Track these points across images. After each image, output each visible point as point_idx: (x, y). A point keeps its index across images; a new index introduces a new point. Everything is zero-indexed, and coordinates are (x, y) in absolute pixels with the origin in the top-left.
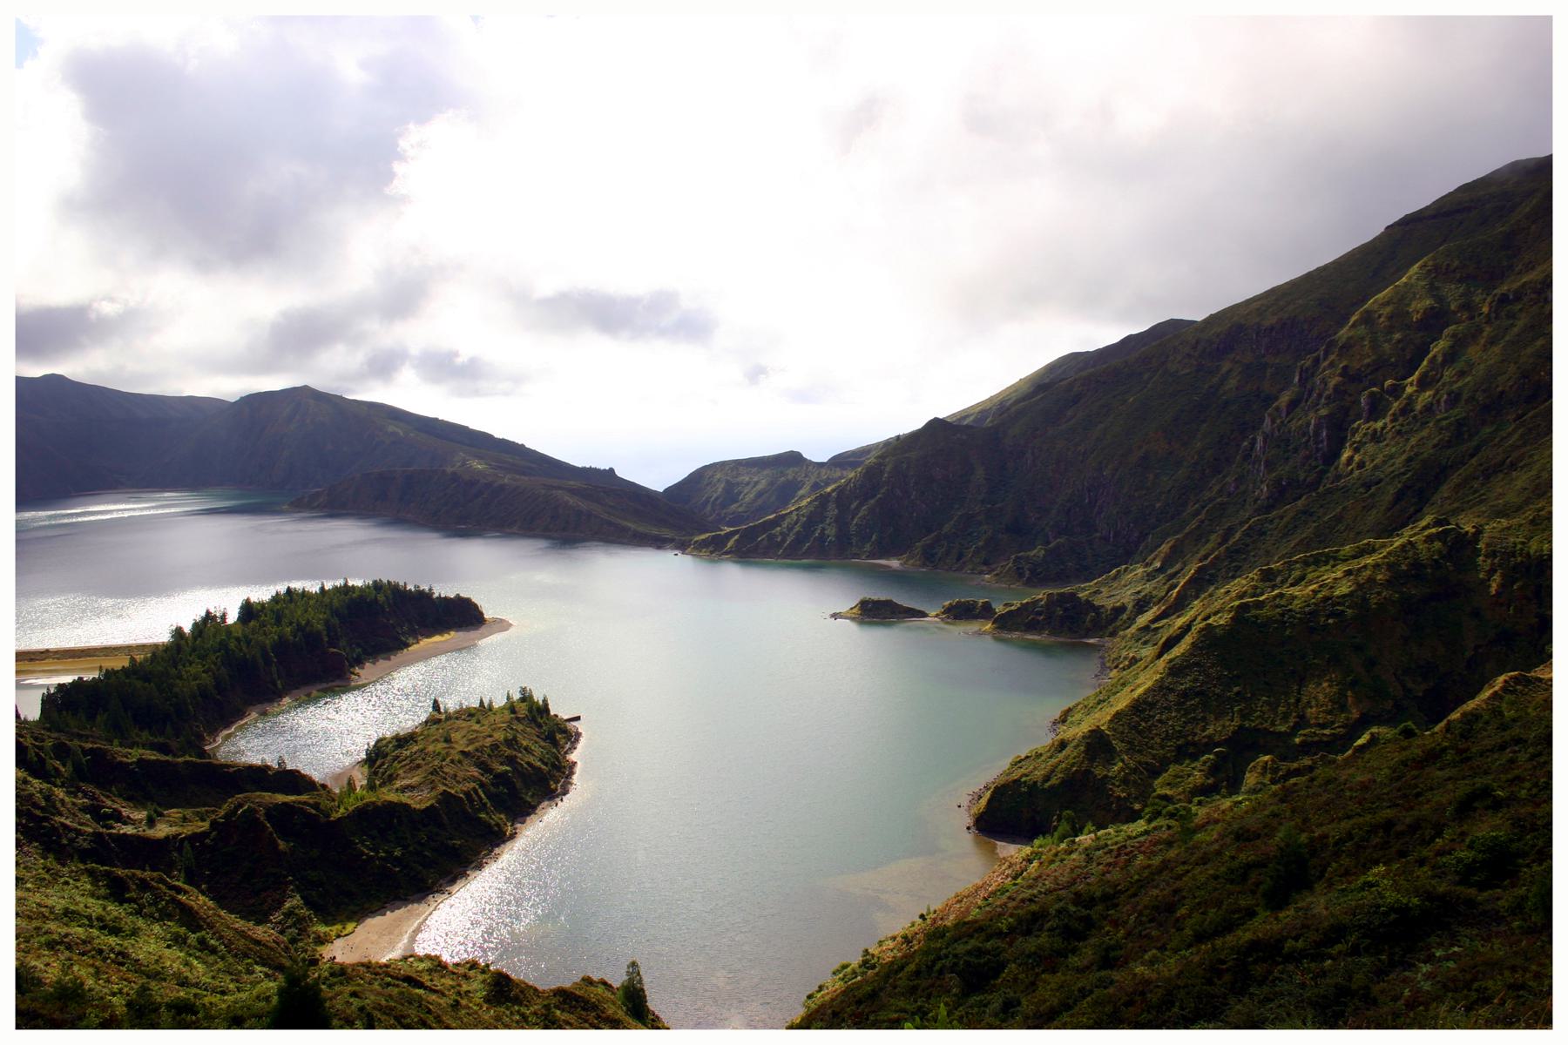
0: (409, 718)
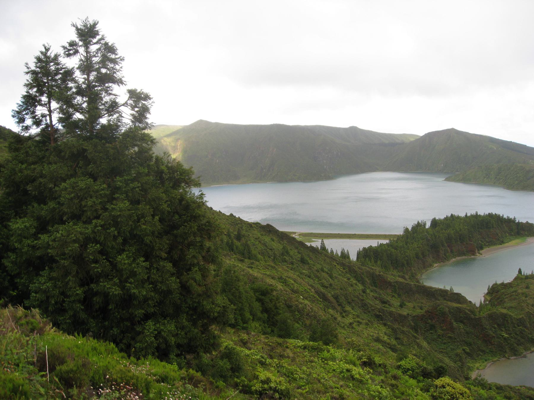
0: (509, 277)
